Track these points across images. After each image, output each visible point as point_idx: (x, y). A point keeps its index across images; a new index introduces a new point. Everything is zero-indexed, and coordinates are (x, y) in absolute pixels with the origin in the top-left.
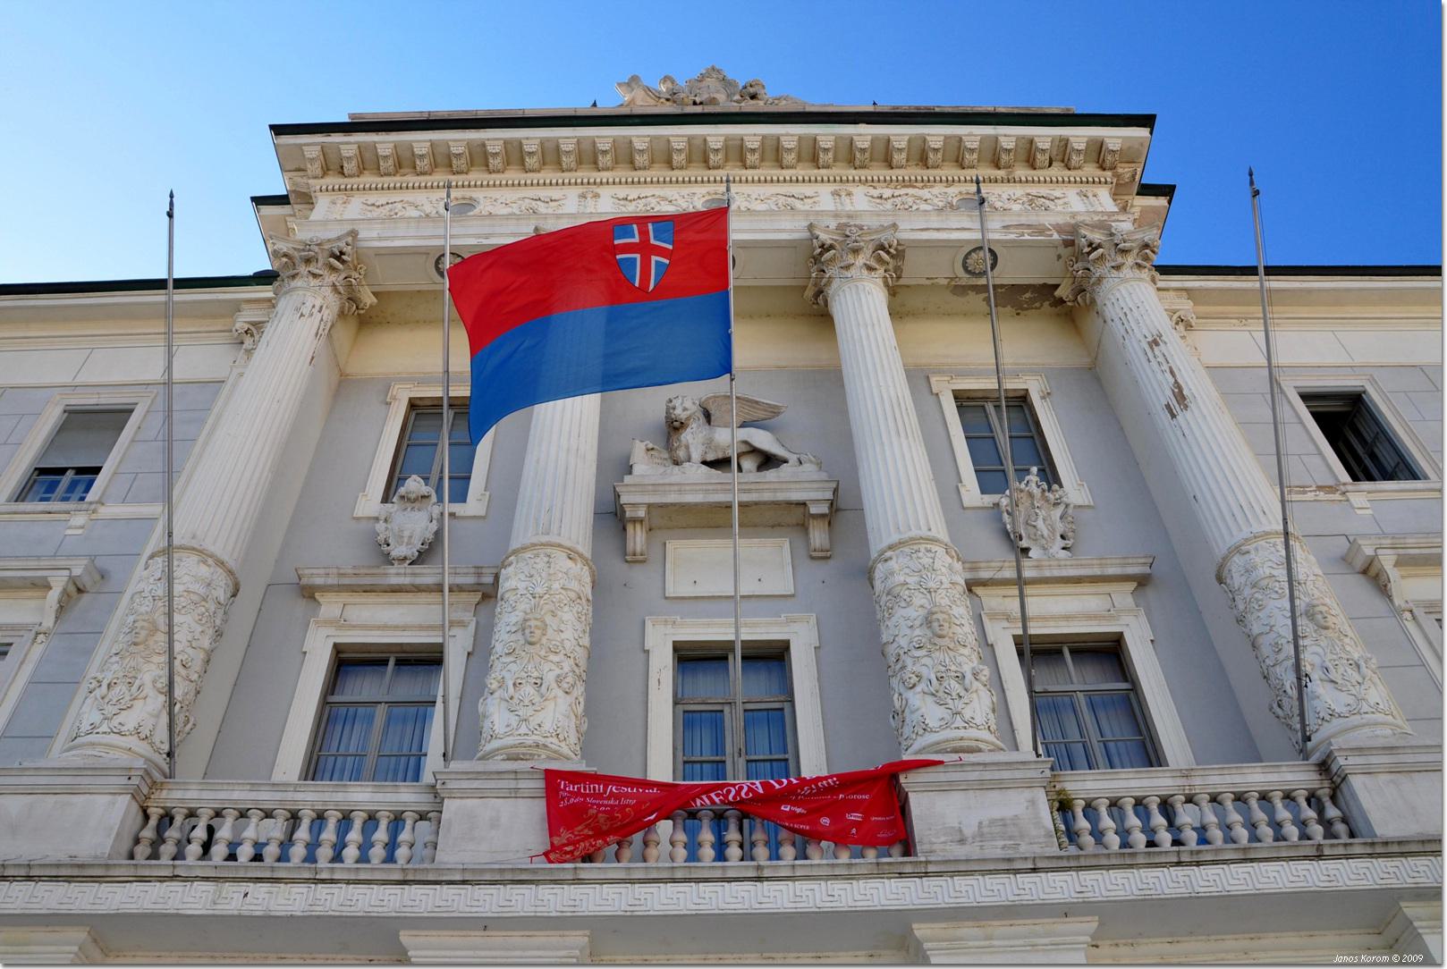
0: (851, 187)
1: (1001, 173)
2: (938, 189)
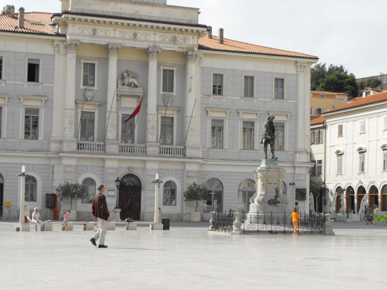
0: (156, 33)
1: (181, 32)
2: (170, 34)
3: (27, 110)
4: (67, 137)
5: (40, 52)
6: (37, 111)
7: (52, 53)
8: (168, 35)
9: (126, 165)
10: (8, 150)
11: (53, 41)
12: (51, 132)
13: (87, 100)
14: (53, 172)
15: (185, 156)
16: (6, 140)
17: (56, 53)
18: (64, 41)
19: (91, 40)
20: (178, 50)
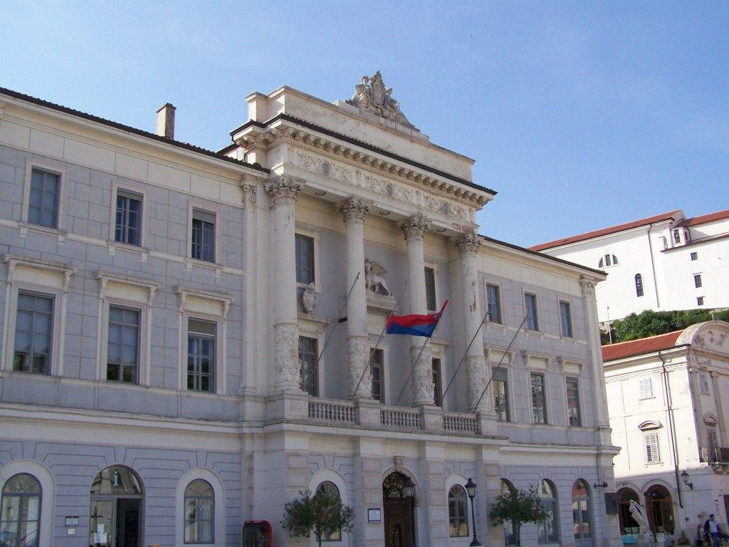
3: (194, 323)
4: (289, 387)
5: (216, 198)
6: (211, 326)
7: (240, 204)
8: (437, 198)
9: (390, 452)
10: (158, 416)
11: (243, 177)
12: (241, 377)
13: (305, 311)
14: (251, 470)
15: (478, 433)
16: (149, 390)
17: (248, 204)
18: (267, 181)
19: (321, 185)
20: (452, 229)
